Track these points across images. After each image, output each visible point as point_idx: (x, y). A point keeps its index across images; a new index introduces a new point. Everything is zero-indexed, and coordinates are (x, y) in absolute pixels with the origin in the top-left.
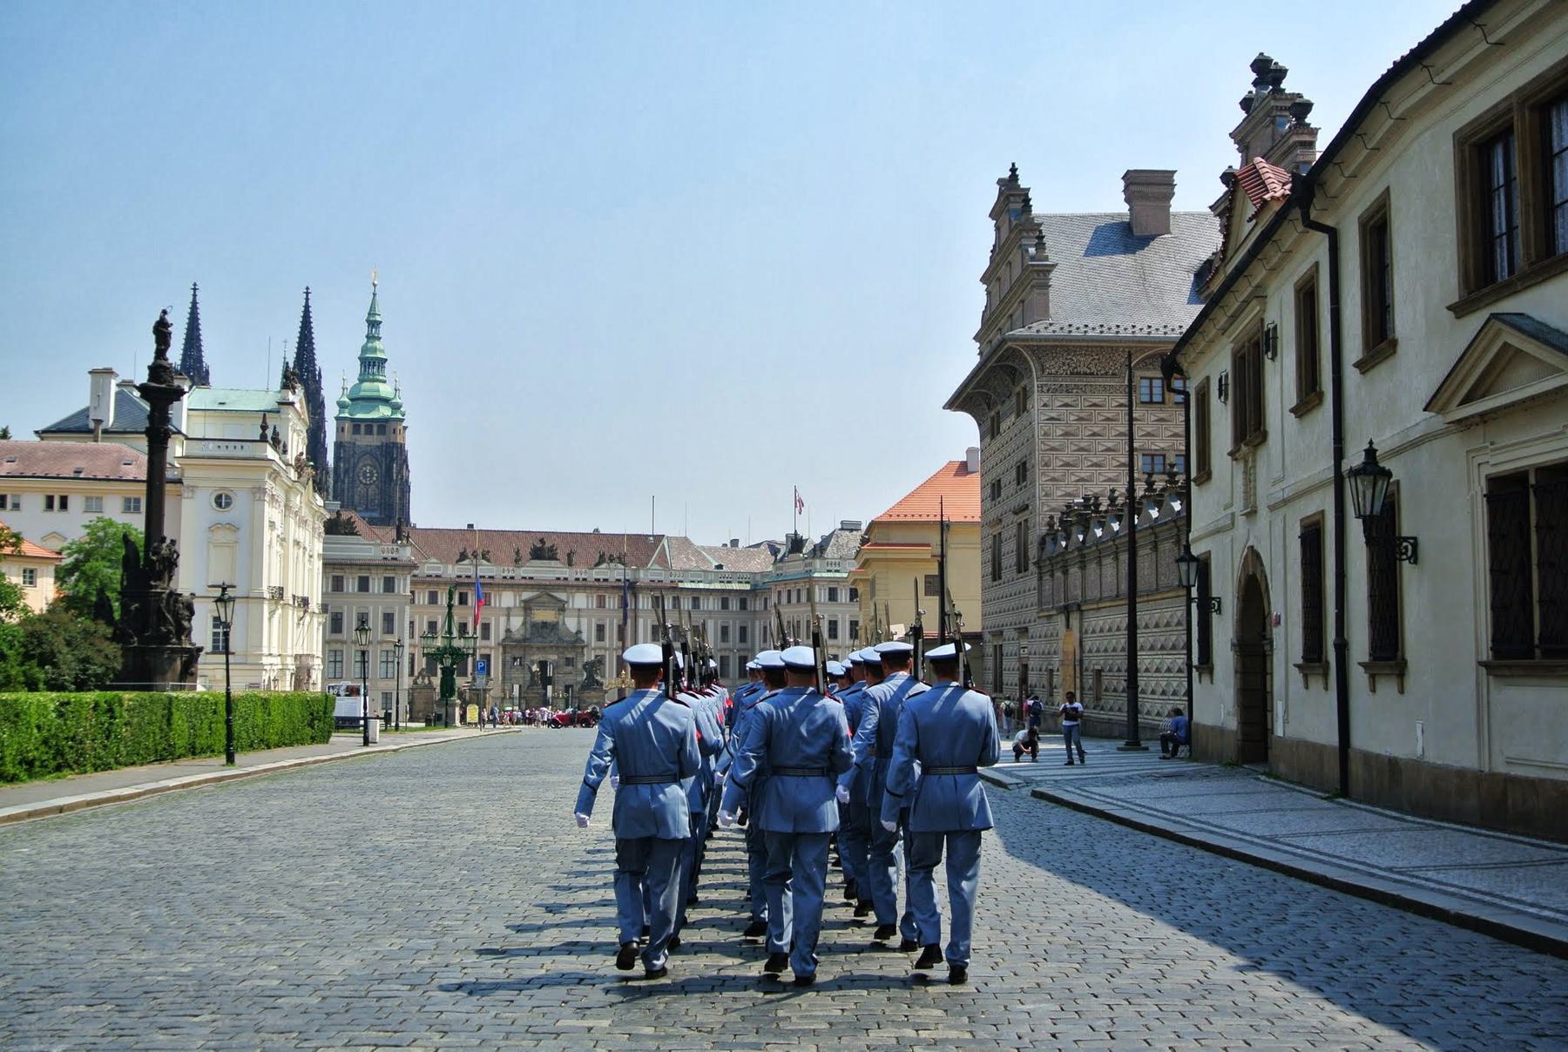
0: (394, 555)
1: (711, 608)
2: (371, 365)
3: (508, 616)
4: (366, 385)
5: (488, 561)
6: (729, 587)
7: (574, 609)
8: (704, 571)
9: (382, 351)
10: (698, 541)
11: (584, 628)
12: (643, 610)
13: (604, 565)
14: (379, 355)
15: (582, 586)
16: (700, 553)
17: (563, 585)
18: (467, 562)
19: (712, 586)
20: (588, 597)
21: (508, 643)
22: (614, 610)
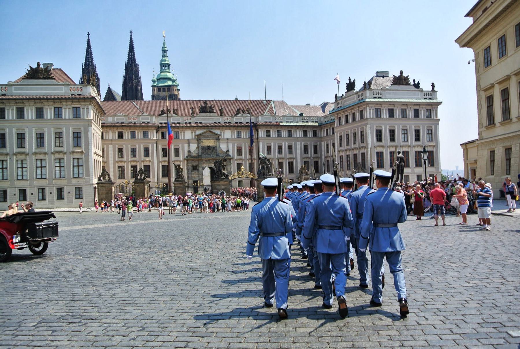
0: (79, 92)
1: (298, 136)
2: (164, 66)
3: (189, 143)
4: (163, 74)
5: (177, 114)
6: (307, 124)
7: (224, 139)
8: (293, 116)
9: (167, 61)
10: (289, 103)
11: (230, 149)
12: (262, 138)
13: (240, 115)
14: (167, 62)
15: (228, 126)
16: (290, 108)
17: (218, 126)
18: (165, 115)
19: (298, 124)
20: (231, 132)
21: (189, 158)
22: (246, 138)
